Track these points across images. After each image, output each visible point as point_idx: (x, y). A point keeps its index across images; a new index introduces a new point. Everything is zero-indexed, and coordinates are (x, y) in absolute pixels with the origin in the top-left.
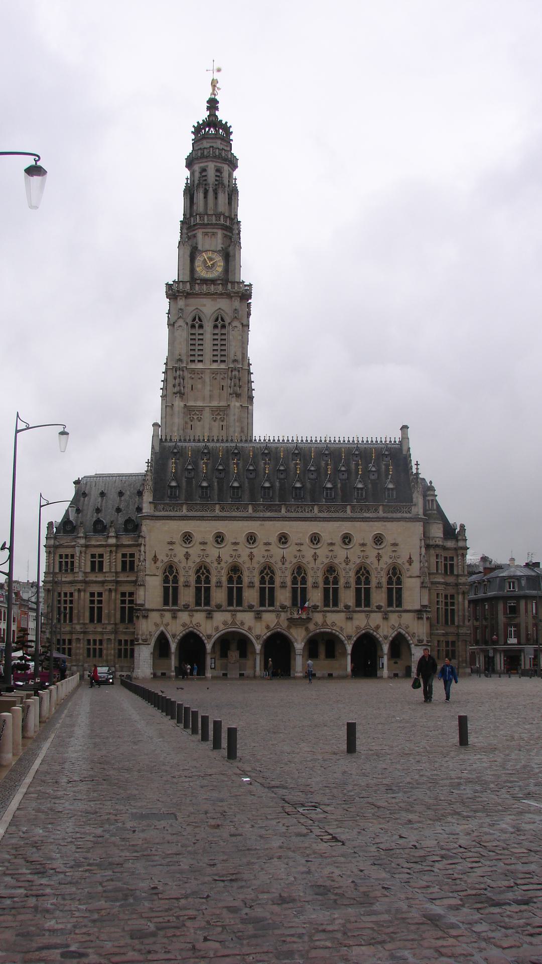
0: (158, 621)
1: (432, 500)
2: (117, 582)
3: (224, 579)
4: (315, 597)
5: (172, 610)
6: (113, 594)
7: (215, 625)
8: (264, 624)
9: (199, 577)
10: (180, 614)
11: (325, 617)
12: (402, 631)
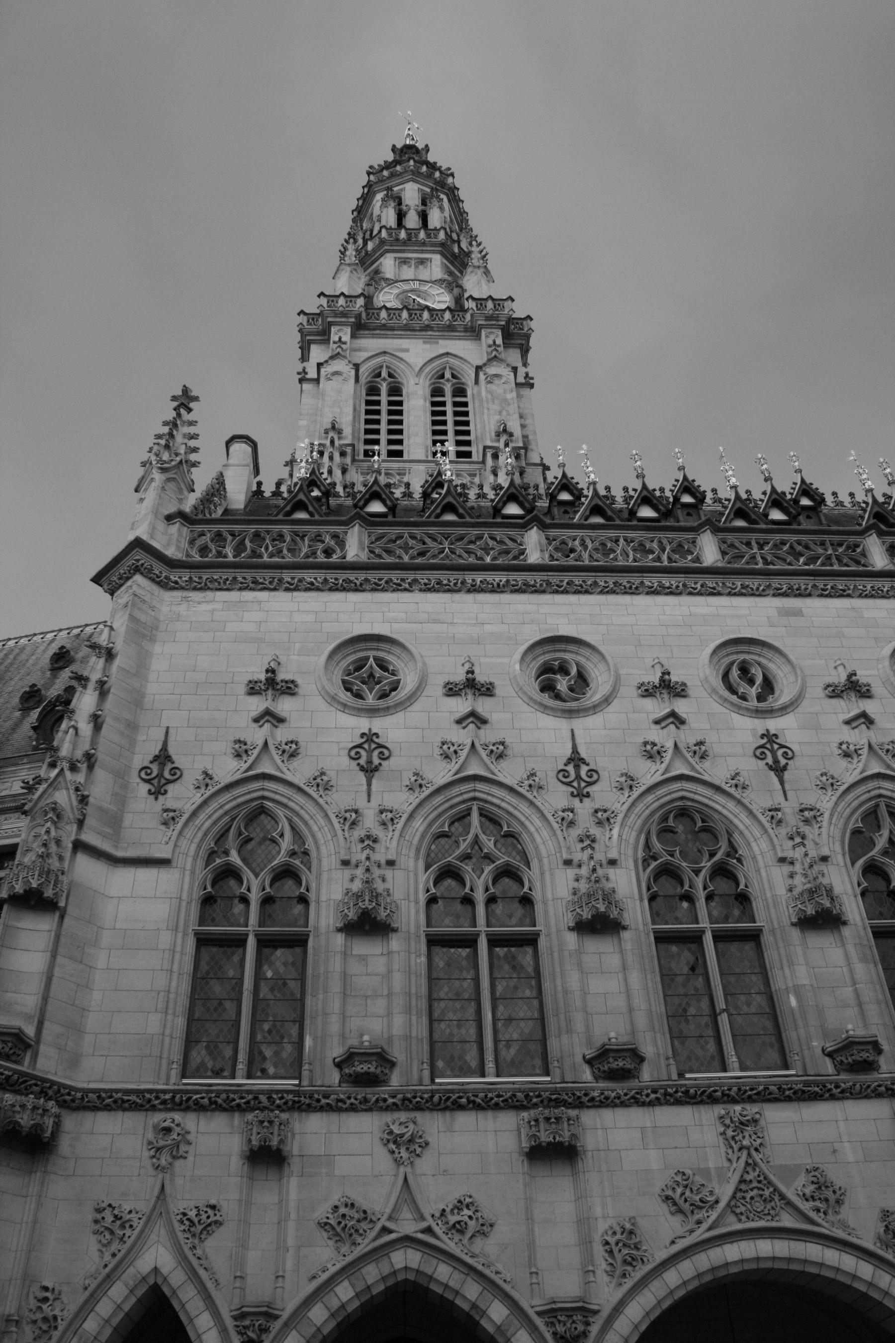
0: (134, 1190)
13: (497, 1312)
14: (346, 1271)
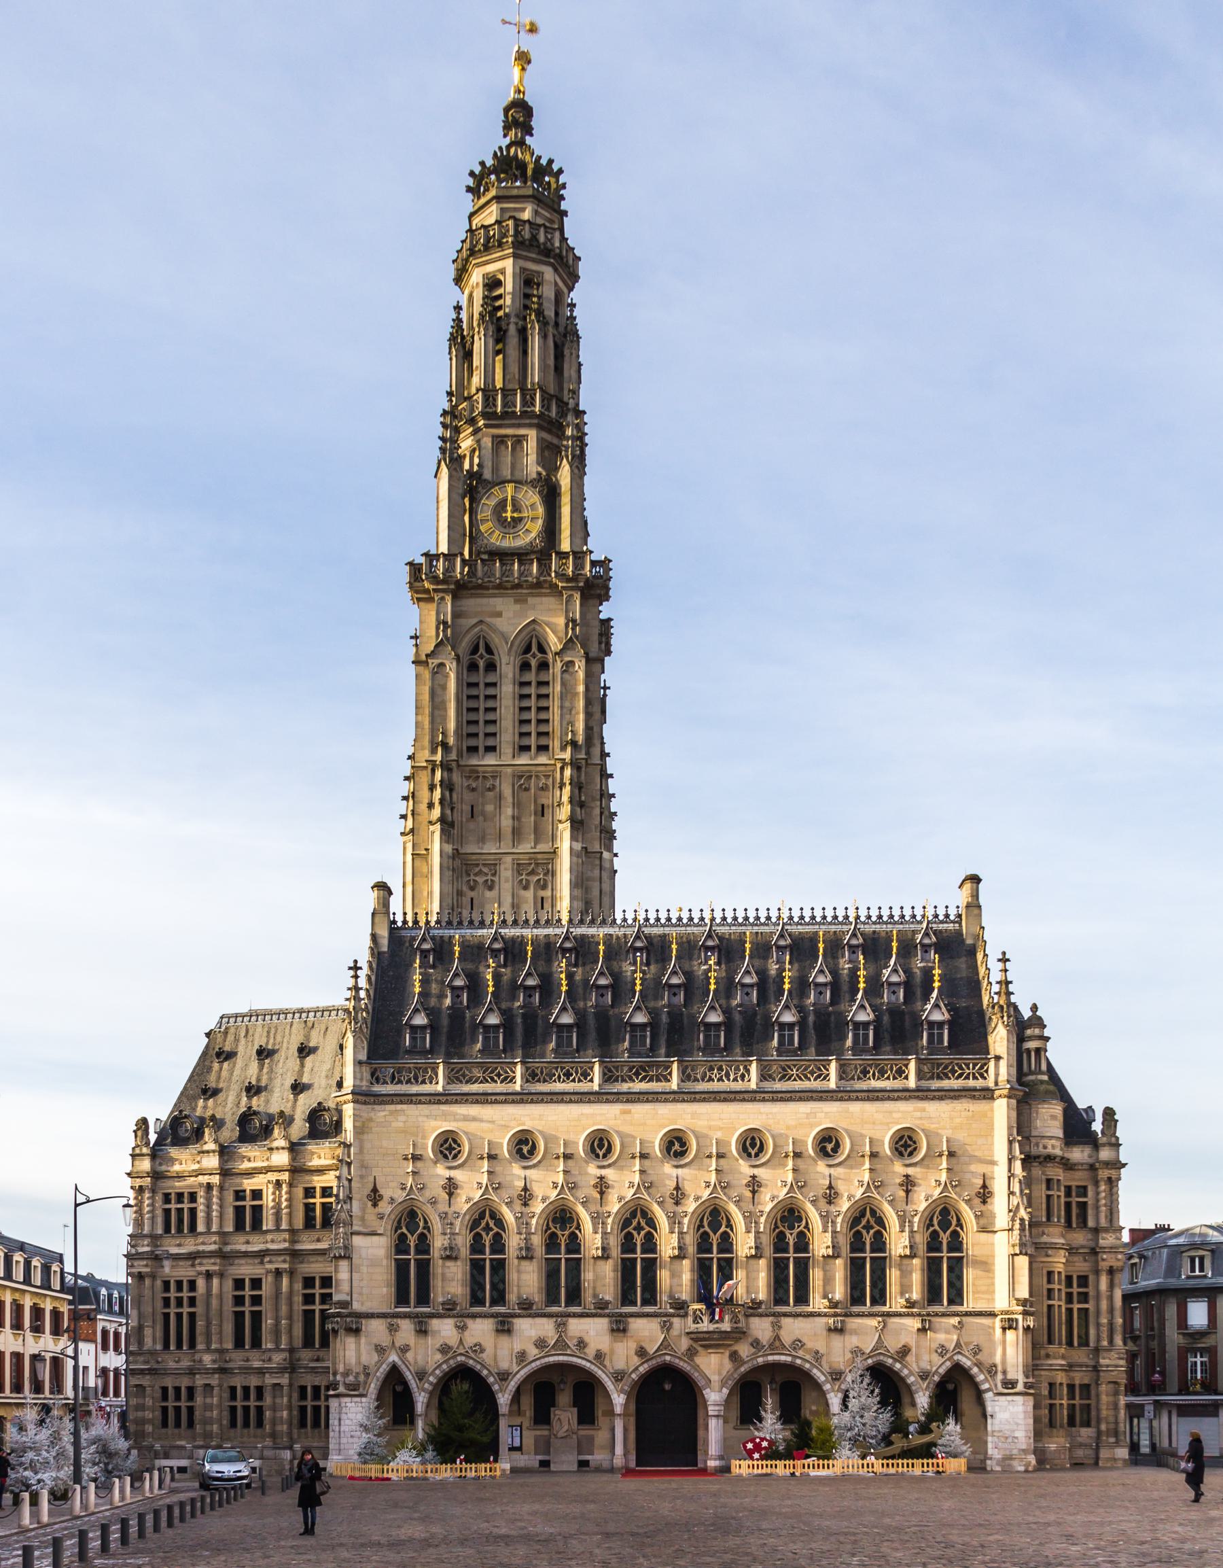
0: (385, 1340)
1: (1038, 1051)
2: (295, 1254)
3: (537, 1241)
4: (752, 1281)
5: (417, 1316)
6: (285, 1281)
7: (518, 1347)
8: (633, 1346)
9: (477, 1238)
10: (435, 1323)
11: (777, 1326)
12: (967, 1363)
13: (485, 1372)
14: (444, 1362)
